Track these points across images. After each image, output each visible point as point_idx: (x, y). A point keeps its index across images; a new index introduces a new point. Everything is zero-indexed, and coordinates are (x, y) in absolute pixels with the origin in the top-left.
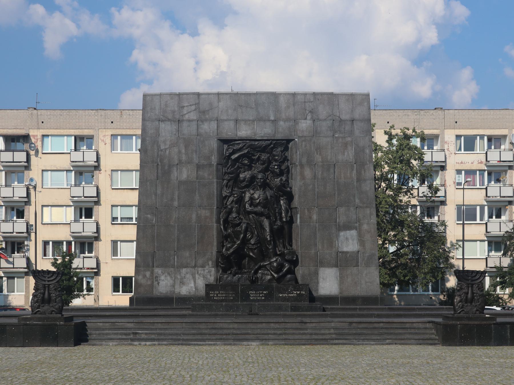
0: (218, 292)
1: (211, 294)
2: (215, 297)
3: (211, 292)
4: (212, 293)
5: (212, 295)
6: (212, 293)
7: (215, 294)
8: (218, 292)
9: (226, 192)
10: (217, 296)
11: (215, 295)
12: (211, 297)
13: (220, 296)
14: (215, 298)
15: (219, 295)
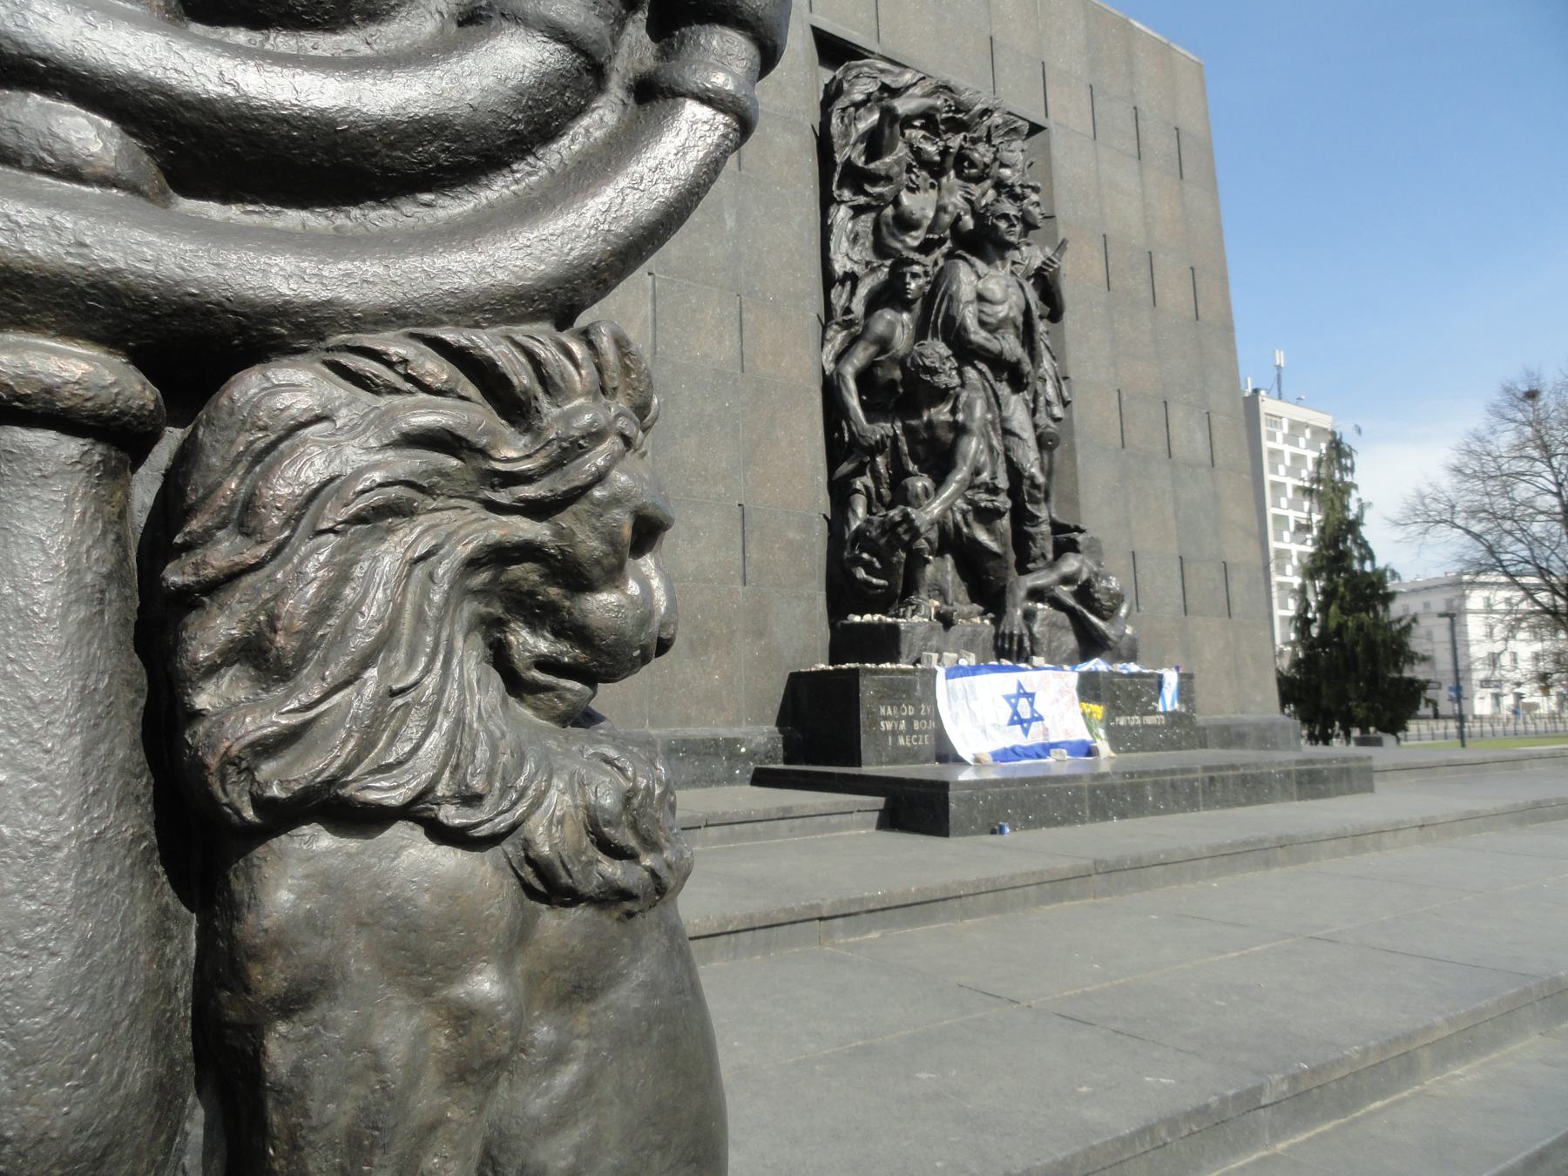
0: (911, 711)
1: (886, 718)
2: (901, 733)
3: (883, 710)
4: (890, 712)
5: (889, 726)
6: (890, 712)
7: (901, 718)
8: (911, 711)
9: (850, 259)
10: (910, 731)
11: (903, 724)
12: (886, 733)
13: (919, 732)
14: (901, 741)
15: (916, 725)
